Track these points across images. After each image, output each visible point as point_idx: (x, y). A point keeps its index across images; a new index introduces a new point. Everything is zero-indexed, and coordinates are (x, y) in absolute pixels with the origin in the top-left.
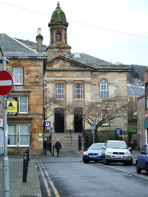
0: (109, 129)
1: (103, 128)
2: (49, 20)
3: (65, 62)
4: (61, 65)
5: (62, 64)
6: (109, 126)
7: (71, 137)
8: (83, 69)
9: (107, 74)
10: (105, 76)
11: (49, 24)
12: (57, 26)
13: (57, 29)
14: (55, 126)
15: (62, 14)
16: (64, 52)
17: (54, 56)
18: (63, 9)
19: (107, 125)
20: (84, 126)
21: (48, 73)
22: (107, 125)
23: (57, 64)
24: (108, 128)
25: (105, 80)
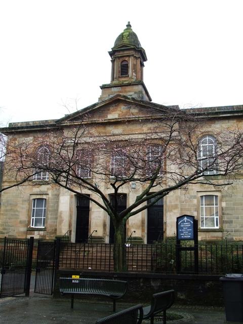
0: (222, 238)
1: (207, 234)
2: (111, 45)
3: (130, 107)
4: (123, 112)
5: (124, 111)
6: (221, 230)
7: (133, 252)
8: (159, 115)
9: (213, 125)
10: (210, 129)
11: (111, 61)
12: (121, 53)
13: (121, 59)
14: (88, 226)
15: (133, 36)
16: (129, 92)
17: (177, 198)
18: (134, 29)
19: (216, 227)
20: (166, 229)
21: (98, 129)
22: (218, 228)
23: (114, 113)
24: (219, 234)
25: (210, 135)
